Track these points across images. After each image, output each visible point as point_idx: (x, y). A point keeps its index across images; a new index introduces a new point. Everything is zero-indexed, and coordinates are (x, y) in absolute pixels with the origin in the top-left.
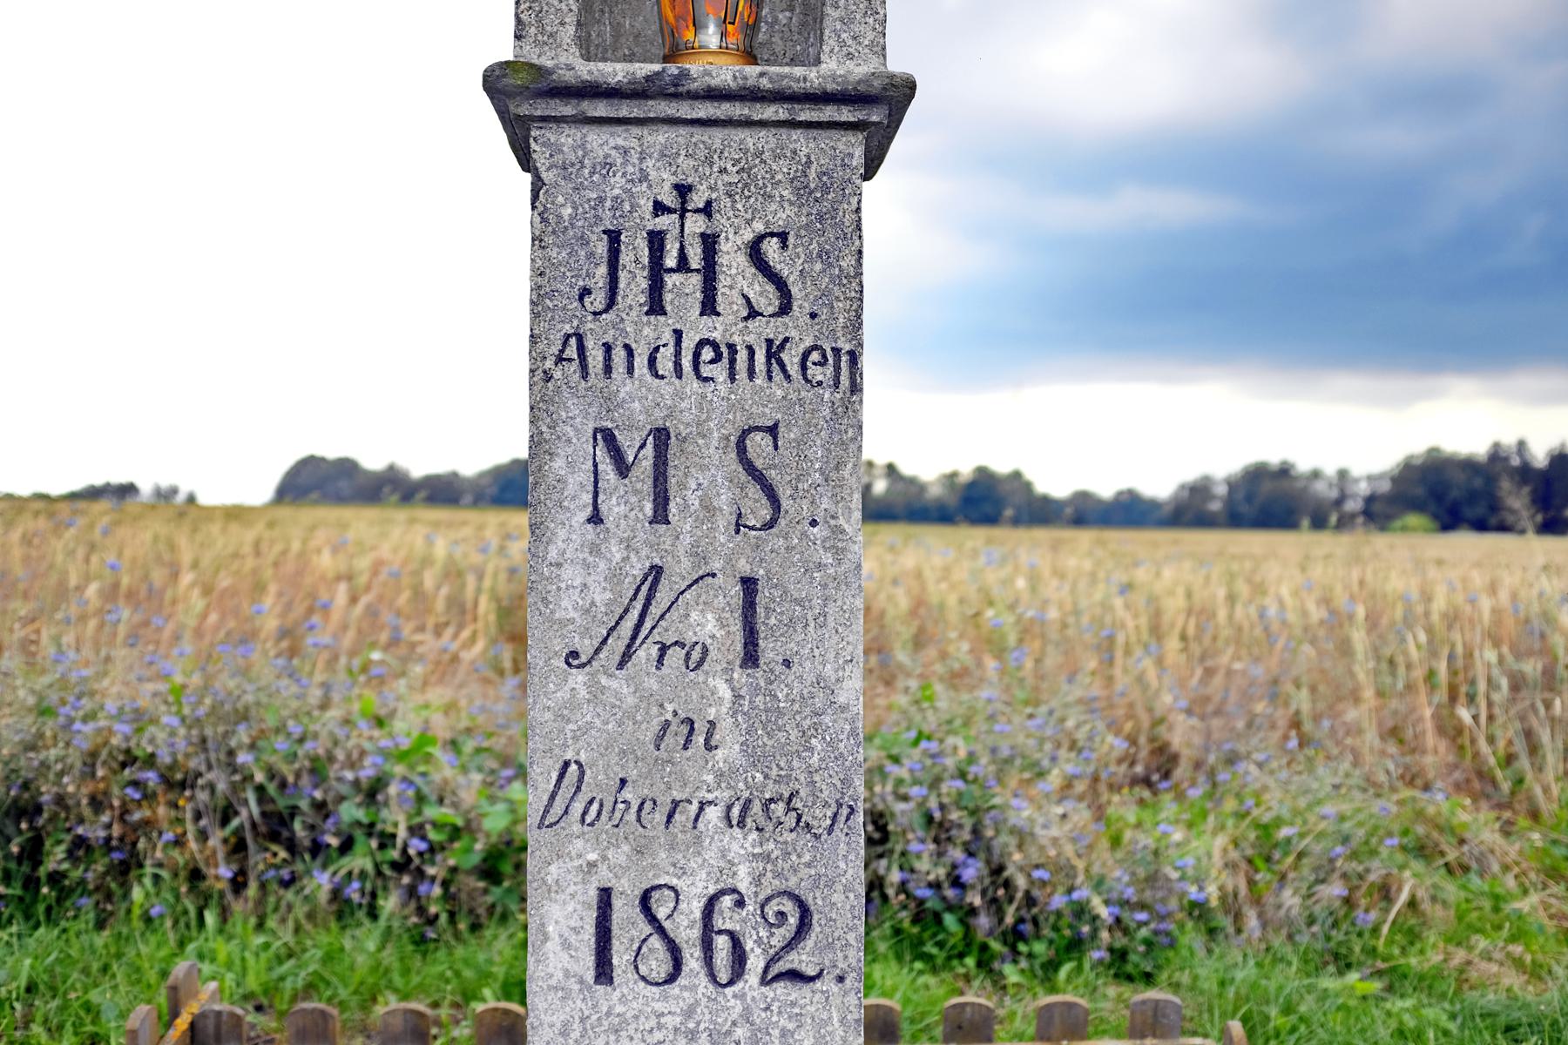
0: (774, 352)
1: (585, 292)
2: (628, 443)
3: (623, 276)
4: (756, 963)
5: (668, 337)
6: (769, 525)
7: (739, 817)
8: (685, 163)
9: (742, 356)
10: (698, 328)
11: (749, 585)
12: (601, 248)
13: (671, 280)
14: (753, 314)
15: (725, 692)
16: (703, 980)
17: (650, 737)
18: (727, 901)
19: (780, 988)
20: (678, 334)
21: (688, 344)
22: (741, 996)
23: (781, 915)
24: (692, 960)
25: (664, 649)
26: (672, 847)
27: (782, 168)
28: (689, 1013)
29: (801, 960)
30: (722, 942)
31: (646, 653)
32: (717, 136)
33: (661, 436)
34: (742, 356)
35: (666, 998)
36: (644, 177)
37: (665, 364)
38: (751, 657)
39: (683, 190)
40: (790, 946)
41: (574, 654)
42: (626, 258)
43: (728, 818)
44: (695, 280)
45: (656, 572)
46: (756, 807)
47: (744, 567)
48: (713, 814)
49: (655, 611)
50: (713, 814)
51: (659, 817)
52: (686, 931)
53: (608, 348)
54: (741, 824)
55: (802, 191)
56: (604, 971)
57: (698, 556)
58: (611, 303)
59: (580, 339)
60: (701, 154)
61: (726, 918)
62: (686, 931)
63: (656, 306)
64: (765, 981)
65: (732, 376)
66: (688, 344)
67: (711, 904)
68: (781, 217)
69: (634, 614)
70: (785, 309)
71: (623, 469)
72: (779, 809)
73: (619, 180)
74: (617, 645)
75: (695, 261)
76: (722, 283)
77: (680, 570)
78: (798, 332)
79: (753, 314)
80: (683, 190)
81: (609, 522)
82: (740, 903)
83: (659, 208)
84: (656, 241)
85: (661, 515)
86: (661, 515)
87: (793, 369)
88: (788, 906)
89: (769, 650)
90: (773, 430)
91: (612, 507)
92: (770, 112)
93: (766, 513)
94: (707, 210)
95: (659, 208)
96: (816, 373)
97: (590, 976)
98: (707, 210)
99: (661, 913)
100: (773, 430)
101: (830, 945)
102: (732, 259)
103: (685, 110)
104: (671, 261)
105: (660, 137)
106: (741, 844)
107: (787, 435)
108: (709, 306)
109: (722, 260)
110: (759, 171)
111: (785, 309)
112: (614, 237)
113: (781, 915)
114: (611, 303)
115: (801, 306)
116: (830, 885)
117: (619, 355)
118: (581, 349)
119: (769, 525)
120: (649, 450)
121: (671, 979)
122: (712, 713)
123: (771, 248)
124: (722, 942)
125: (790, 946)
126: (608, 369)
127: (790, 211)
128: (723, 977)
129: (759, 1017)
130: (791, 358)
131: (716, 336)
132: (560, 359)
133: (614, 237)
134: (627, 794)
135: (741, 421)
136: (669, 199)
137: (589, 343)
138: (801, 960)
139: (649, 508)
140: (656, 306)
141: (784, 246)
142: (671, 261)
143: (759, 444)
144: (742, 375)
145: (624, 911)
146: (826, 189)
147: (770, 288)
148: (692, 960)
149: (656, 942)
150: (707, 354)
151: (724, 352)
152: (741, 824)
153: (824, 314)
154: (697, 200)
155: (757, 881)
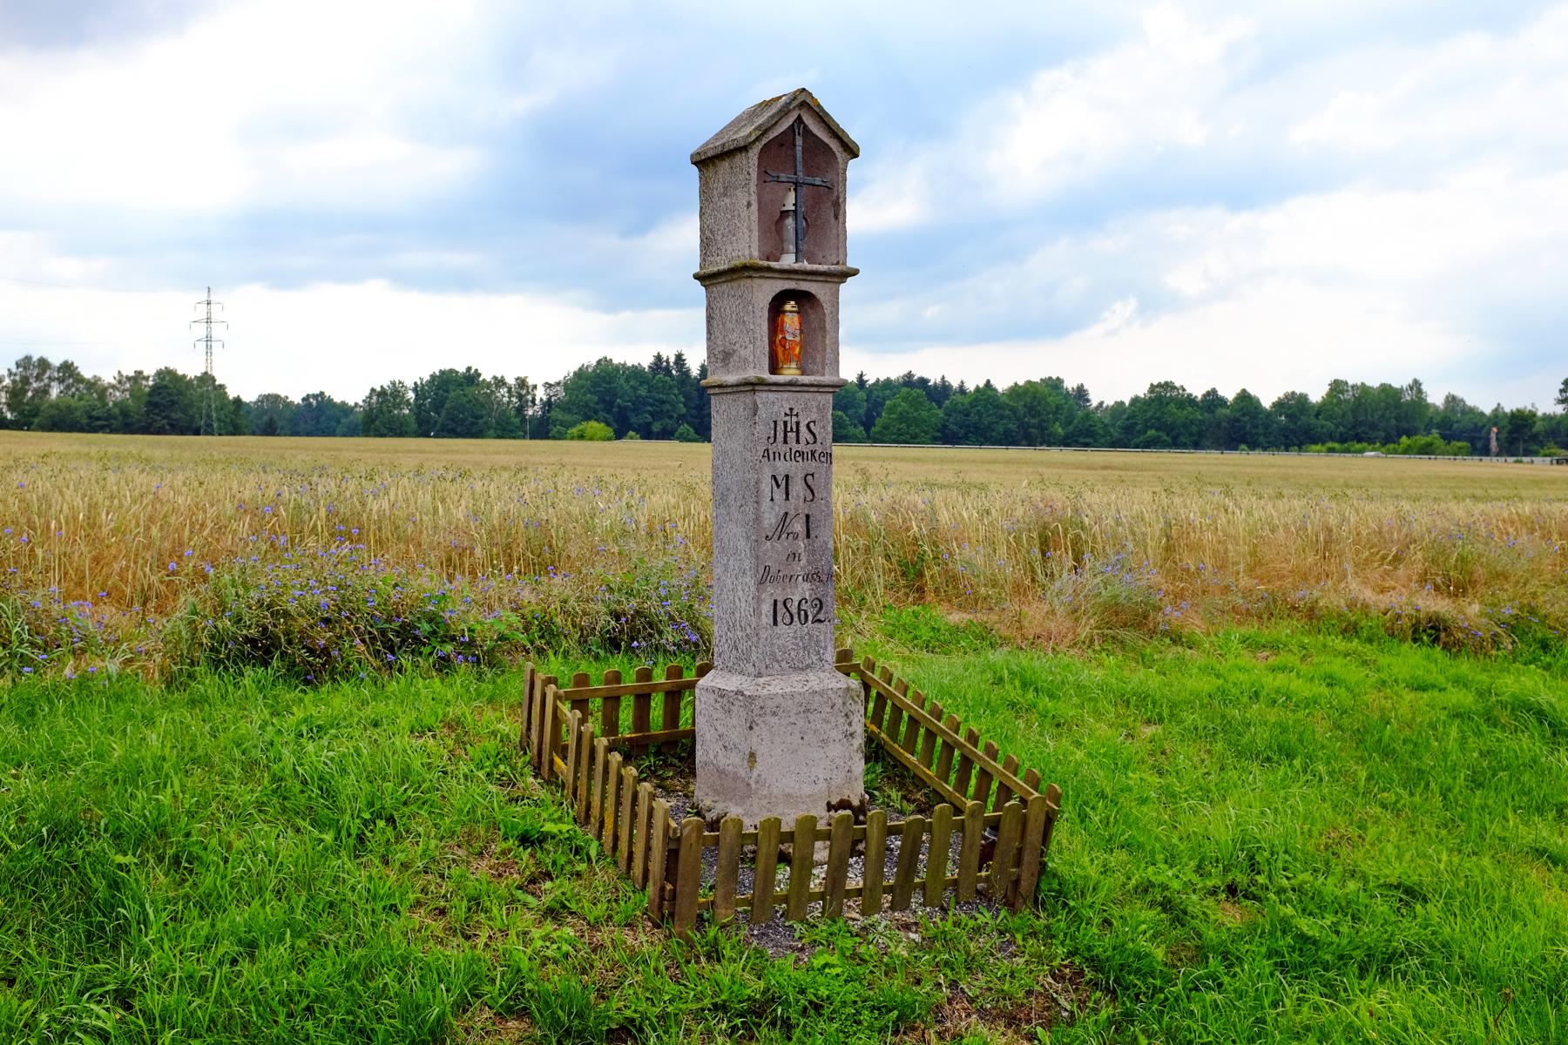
0: (813, 453)
2: (780, 479)
4: (810, 618)
6: (812, 500)
10: (796, 447)
11: (808, 517)
12: (773, 426)
13: (789, 434)
14: (808, 443)
17: (784, 559)
21: (793, 452)
24: (796, 619)
27: (814, 404)
28: (795, 632)
29: (821, 617)
32: (799, 395)
33: (787, 477)
37: (788, 458)
38: (808, 536)
39: (791, 409)
40: (818, 613)
44: (794, 434)
45: (786, 513)
47: (806, 512)
48: (800, 578)
50: (800, 578)
52: (794, 610)
56: (775, 623)
57: (796, 509)
62: (794, 610)
63: (785, 442)
66: (793, 452)
67: (800, 602)
68: (814, 417)
70: (815, 442)
71: (778, 486)
74: (778, 533)
75: (794, 429)
76: (801, 435)
77: (792, 513)
79: (808, 443)
80: (791, 409)
83: (786, 414)
84: (785, 423)
85: (787, 498)
86: (787, 498)
89: (812, 536)
90: (812, 475)
91: (776, 497)
94: (797, 415)
95: (786, 414)
96: (822, 459)
98: (797, 415)
100: (812, 475)
102: (803, 429)
105: (786, 395)
106: (807, 586)
107: (816, 476)
108: (798, 442)
111: (815, 442)
112: (775, 422)
115: (819, 441)
117: (777, 455)
119: (812, 500)
121: (791, 623)
123: (812, 425)
125: (818, 613)
130: (817, 455)
133: (775, 422)
135: (805, 472)
136: (788, 412)
140: (785, 442)
143: (810, 477)
145: (780, 605)
148: (796, 619)
151: (802, 454)
154: (795, 413)
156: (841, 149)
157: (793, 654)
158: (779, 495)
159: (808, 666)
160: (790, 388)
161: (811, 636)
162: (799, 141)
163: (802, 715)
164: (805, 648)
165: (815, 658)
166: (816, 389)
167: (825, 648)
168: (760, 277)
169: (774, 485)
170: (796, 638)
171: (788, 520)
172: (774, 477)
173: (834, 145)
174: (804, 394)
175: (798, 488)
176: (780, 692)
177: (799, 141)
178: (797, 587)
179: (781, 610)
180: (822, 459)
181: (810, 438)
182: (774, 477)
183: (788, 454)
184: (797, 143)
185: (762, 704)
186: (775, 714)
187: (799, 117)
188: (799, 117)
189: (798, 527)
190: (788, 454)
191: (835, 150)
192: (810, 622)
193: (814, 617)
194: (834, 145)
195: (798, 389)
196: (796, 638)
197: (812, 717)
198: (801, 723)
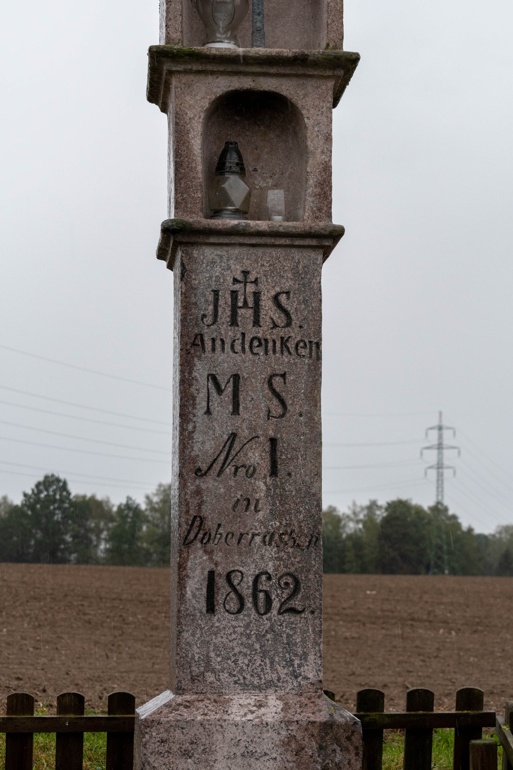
0: (284, 342)
1: (204, 316)
2: (222, 380)
3: (220, 310)
4: (276, 604)
5: (239, 336)
6: (282, 416)
8: (247, 262)
9: (270, 345)
10: (251, 332)
11: (273, 441)
12: (211, 298)
13: (240, 312)
14: (275, 326)
15: (263, 487)
16: (253, 611)
17: (231, 505)
18: (264, 577)
19: (286, 616)
20: (243, 334)
21: (248, 339)
23: (287, 584)
24: (249, 604)
26: (240, 554)
27: (288, 265)
28: (247, 626)
29: (297, 603)
30: (261, 595)
31: (229, 470)
32: (260, 251)
33: (236, 378)
34: (270, 345)
35: (237, 619)
36: (229, 268)
38: (274, 472)
39: (246, 273)
40: (291, 597)
41: (199, 470)
42: (221, 302)
43: (264, 542)
44: (250, 312)
45: (233, 436)
46: (276, 537)
47: (271, 433)
48: (258, 539)
49: (233, 452)
50: (258, 539)
51: (235, 541)
53: (213, 340)
54: (270, 544)
55: (296, 274)
56: (211, 609)
57: (250, 428)
59: (202, 335)
60: (253, 258)
61: (264, 585)
63: (234, 322)
64: (280, 613)
65: (266, 352)
67: (257, 579)
68: (287, 285)
69: (224, 454)
70: (289, 324)
71: (220, 391)
72: (286, 538)
73: (218, 269)
74: (217, 467)
75: (251, 303)
76: (262, 313)
77: (245, 433)
79: (275, 326)
80: (246, 273)
81: (215, 414)
82: (269, 578)
84: (234, 294)
85: (236, 411)
86: (236, 411)
87: (292, 350)
88: (290, 580)
90: (283, 376)
91: (215, 406)
92: (282, 241)
93: (280, 411)
94: (256, 282)
95: (235, 281)
96: (302, 352)
97: (204, 610)
98: (256, 282)
99: (236, 582)
100: (283, 376)
101: (308, 598)
104: (240, 304)
105: (236, 251)
106: (271, 551)
107: (290, 378)
108: (256, 323)
109: (262, 303)
110: (278, 266)
111: (289, 324)
112: (216, 293)
113: (287, 584)
117: (218, 343)
118: (202, 341)
119: (282, 416)
120: (231, 384)
121: (239, 611)
122: (257, 496)
123: (283, 298)
124: (261, 595)
125: (291, 597)
126: (214, 349)
127: (291, 283)
128: (262, 611)
129: (277, 628)
130: (291, 345)
132: (194, 344)
133: (216, 293)
134: (221, 531)
135: (269, 371)
136: (240, 277)
137: (206, 338)
138: (297, 603)
139: (231, 407)
140: (234, 322)
141: (288, 298)
142: (240, 304)
143: (277, 381)
144: (271, 352)
145: (221, 582)
146: (306, 273)
147: (283, 315)
148: (249, 604)
149: (233, 595)
150: (256, 343)
151: (263, 342)
152: (270, 544)
153: (305, 327)
154: (252, 277)
155: (276, 569)
157: (242, 661)
159: (270, 684)
160: (241, 240)
161: (277, 636)
163: (239, 760)
164: (264, 654)
165: (283, 672)
166: (288, 242)
167: (304, 656)
168: (186, 72)
170: (249, 636)
171: (237, 446)
172: (213, 378)
174: (269, 250)
176: (199, 718)
178: (249, 553)
180: (302, 352)
181: (280, 318)
182: (213, 378)
183: (238, 342)
185: (165, 736)
186: (187, 754)
192: (275, 612)
193: (282, 604)
195: (254, 241)
196: (249, 636)
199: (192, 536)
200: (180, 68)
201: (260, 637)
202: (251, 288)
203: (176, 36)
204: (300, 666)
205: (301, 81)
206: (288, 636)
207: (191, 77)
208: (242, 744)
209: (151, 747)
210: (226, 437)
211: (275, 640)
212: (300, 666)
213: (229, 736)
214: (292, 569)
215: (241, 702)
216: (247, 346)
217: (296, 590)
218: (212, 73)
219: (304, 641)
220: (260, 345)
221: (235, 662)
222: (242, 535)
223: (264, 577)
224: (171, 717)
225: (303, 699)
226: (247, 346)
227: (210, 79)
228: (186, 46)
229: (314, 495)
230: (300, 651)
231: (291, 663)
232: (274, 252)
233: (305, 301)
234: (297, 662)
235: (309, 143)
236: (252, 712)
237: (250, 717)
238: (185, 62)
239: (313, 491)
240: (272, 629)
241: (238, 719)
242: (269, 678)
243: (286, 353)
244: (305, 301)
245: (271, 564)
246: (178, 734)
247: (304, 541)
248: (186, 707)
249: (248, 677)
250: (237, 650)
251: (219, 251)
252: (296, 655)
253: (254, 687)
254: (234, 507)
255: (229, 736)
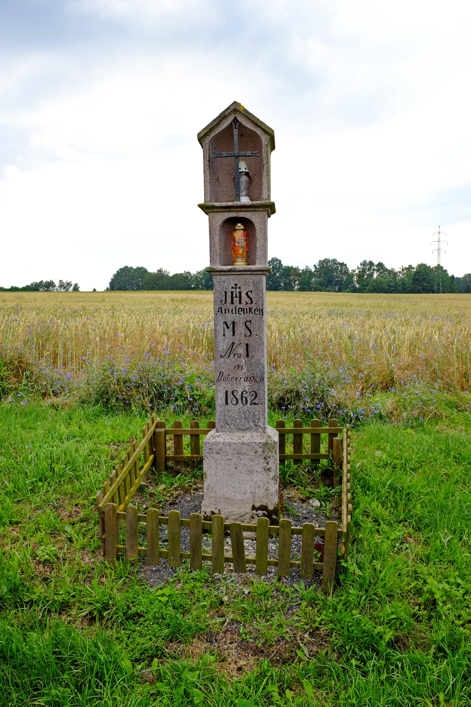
0: (250, 309)
1: (222, 301)
2: (229, 324)
3: (227, 298)
4: (249, 402)
5: (234, 308)
6: (250, 336)
7: (246, 379)
8: (236, 281)
9: (245, 310)
10: (239, 306)
11: (247, 345)
12: (224, 294)
13: (234, 299)
14: (247, 304)
15: (244, 361)
16: (241, 404)
17: (233, 368)
18: (245, 392)
19: (253, 405)
20: (236, 307)
21: (237, 309)
22: (247, 407)
23: (253, 394)
25: (235, 355)
26: (236, 385)
28: (239, 409)
29: (256, 401)
30: (244, 399)
31: (232, 355)
32: (241, 276)
33: (234, 323)
34: (245, 310)
35: (236, 407)
36: (230, 283)
37: (234, 312)
38: (248, 356)
39: (236, 285)
40: (254, 399)
41: (221, 356)
42: (227, 296)
43: (245, 380)
44: (238, 299)
45: (233, 343)
46: (249, 378)
47: (246, 342)
48: (242, 379)
49: (233, 349)
50: (242, 379)
51: (234, 380)
52: (239, 397)
53: (225, 309)
54: (247, 381)
55: (254, 284)
56: (227, 403)
57: (239, 341)
58: (226, 302)
59: (221, 308)
60: (239, 279)
61: (245, 395)
62: (239, 397)
63: (232, 303)
64: (250, 404)
65: (244, 313)
66: (237, 309)
68: (251, 288)
69: (230, 350)
70: (252, 303)
71: (228, 328)
72: (252, 379)
73: (226, 284)
74: (228, 354)
75: (238, 296)
76: (242, 299)
77: (237, 342)
78: (254, 306)
79: (247, 304)
80: (236, 285)
81: (226, 336)
82: (247, 393)
83: (232, 288)
84: (232, 293)
85: (234, 334)
86: (234, 334)
87: (253, 312)
88: (254, 393)
89: (250, 355)
90: (250, 321)
91: (226, 334)
92: (248, 273)
93: (249, 334)
94: (240, 288)
95: (232, 288)
96: (256, 312)
97: (225, 404)
98: (240, 288)
99: (235, 394)
100: (250, 321)
101: (260, 399)
102: (244, 295)
103: (236, 273)
104: (234, 296)
105: (232, 277)
106: (247, 384)
107: (252, 322)
108: (240, 303)
109: (242, 295)
110: (247, 282)
111: (252, 303)
112: (226, 292)
113: (253, 394)
114: (226, 302)
115: (254, 302)
116: (260, 390)
117: (227, 310)
118: (221, 310)
119: (250, 336)
120: (232, 325)
121: (237, 404)
122: (242, 364)
123: (249, 293)
124: (244, 399)
125: (254, 399)
126: (225, 313)
127: (252, 288)
128: (244, 404)
129: (250, 410)
130: (253, 310)
131: (241, 307)
132: (218, 311)
133: (226, 292)
134: (230, 376)
135: (245, 320)
136: (234, 286)
137: (222, 309)
138: (256, 401)
139: (232, 333)
140: (232, 303)
141: (251, 293)
142: (234, 296)
143: (248, 323)
144: (245, 313)
145: (230, 394)
146: (257, 284)
147: (249, 300)
149: (234, 399)
150: (240, 310)
151: (243, 310)
152: (247, 381)
153: (258, 303)
154: (238, 286)
155: (249, 389)
156: (263, 133)
158: (229, 333)
159: (247, 429)
160: (233, 273)
161: (250, 412)
162: (236, 132)
163: (236, 455)
164: (245, 418)
165: (252, 425)
166: (250, 273)
169: (226, 327)
170: (240, 413)
171: (234, 347)
172: (226, 323)
173: (258, 131)
174: (244, 276)
175: (240, 329)
176: (222, 441)
177: (236, 132)
179: (230, 396)
181: (248, 301)
182: (226, 323)
183: (234, 310)
184: (234, 134)
185: (211, 447)
186: (218, 453)
187: (235, 120)
188: (235, 120)
189: (241, 350)
190: (234, 310)
191: (259, 134)
192: (249, 404)
194: (258, 131)
195: (238, 273)
196: (240, 413)
197: (242, 457)
198: (235, 460)
199: (219, 379)
200: (210, 211)
201: (244, 413)
202: (238, 290)
203: (208, 199)
204: (257, 422)
205: (254, 213)
206: (253, 412)
207: (214, 214)
208: (237, 450)
209: (206, 451)
210: (230, 343)
211: (249, 414)
212: (257, 422)
213: (232, 447)
214: (254, 390)
215: (237, 435)
216: (237, 311)
217: (256, 396)
218: (221, 212)
219: (259, 414)
220: (242, 311)
221: (236, 421)
222: (237, 378)
223: (245, 392)
224: (213, 441)
225: (258, 434)
226: (237, 311)
227: (221, 213)
228: (211, 204)
229: (262, 363)
230: (258, 417)
231: (254, 421)
232: (246, 277)
233: (257, 294)
234: (257, 421)
235: (257, 236)
236: (240, 439)
237: (239, 441)
238: (211, 209)
239: (261, 362)
240: (248, 410)
241: (235, 441)
242: (247, 426)
243: (251, 313)
244: (257, 294)
245: (247, 388)
246: (215, 447)
247: (258, 380)
248: (218, 437)
249: (240, 426)
250: (236, 417)
251: (226, 277)
252: (256, 419)
253: (242, 430)
254: (234, 368)
255: (232, 447)
